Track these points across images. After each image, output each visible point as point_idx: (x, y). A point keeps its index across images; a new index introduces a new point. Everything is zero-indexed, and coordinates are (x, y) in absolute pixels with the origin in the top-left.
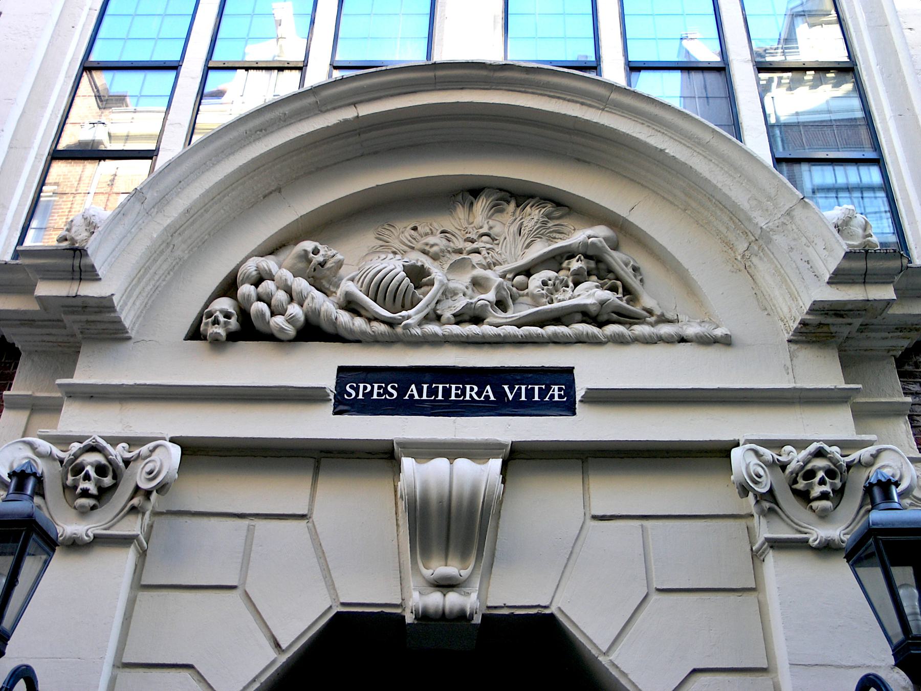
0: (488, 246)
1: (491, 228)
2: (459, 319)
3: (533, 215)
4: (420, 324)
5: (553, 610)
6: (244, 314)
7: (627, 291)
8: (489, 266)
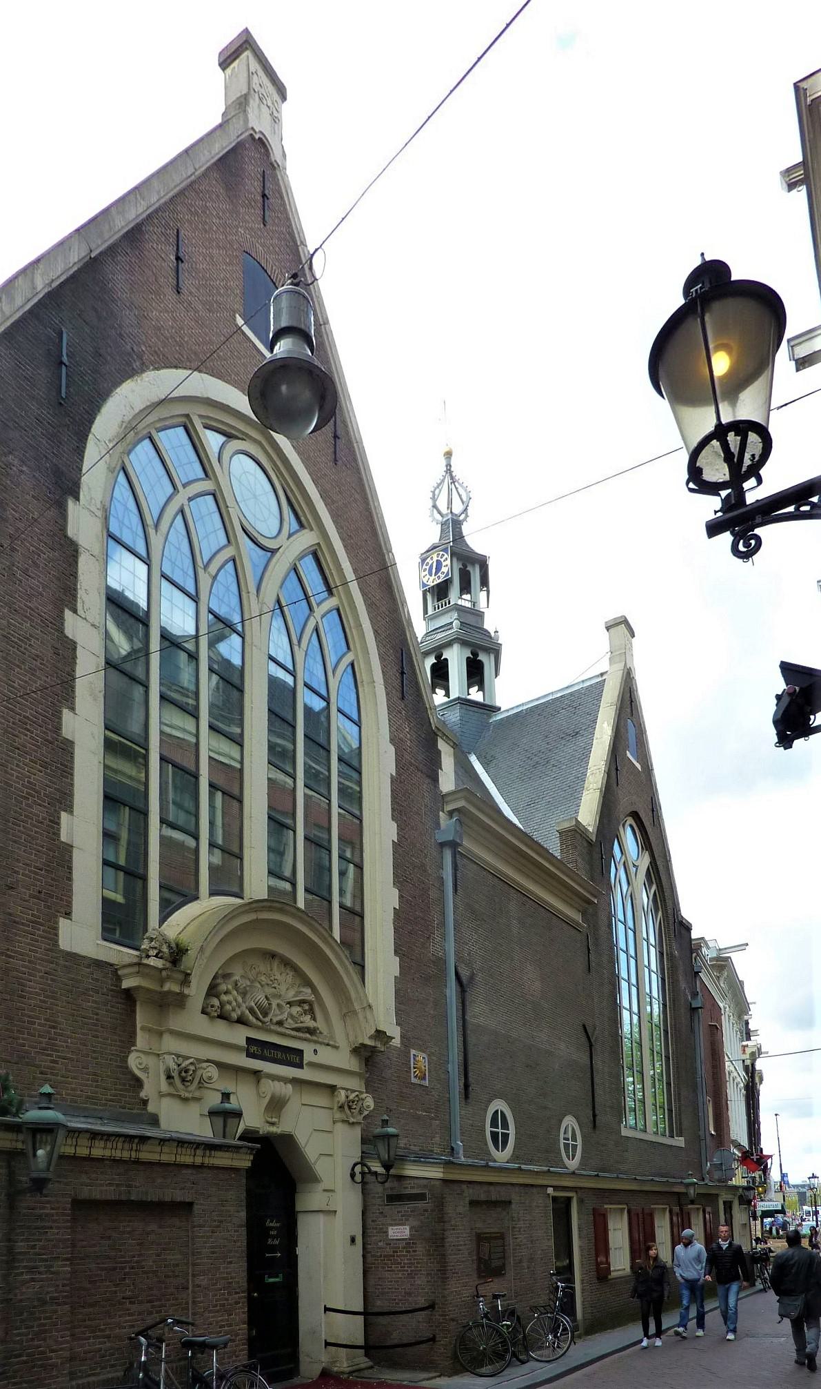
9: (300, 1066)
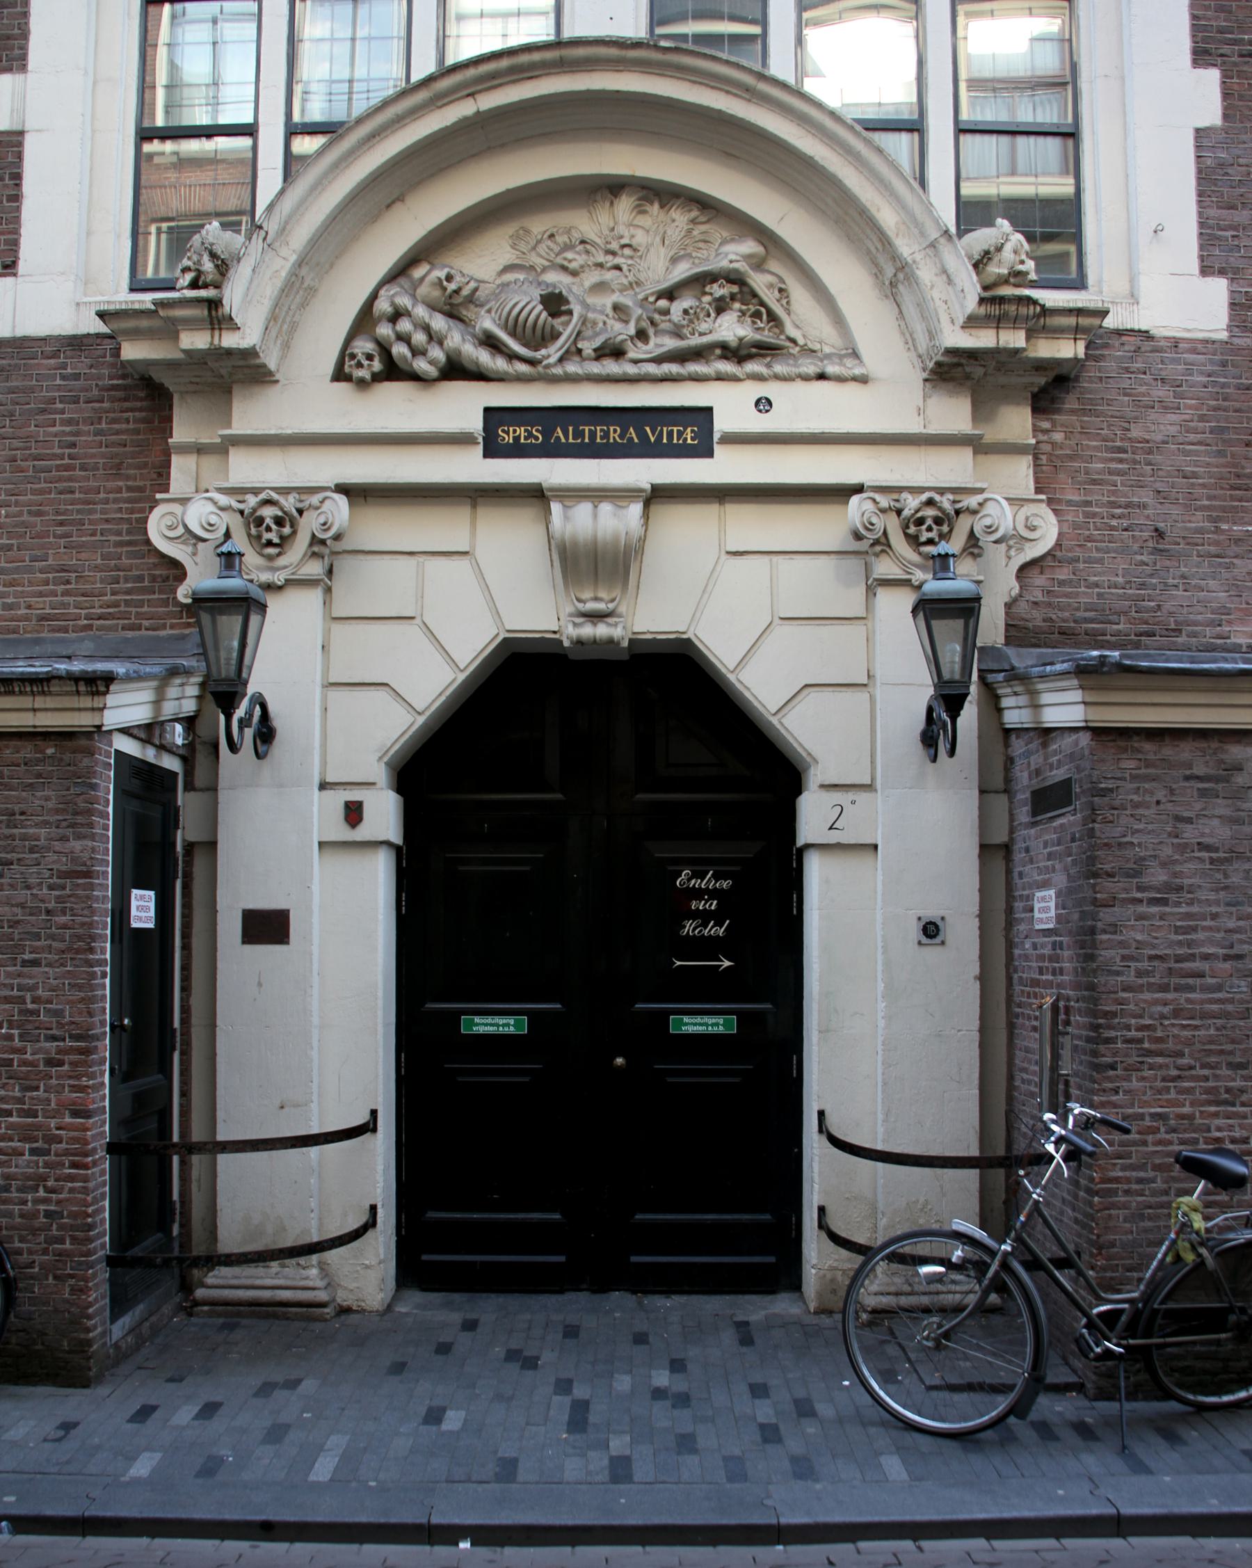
0: (630, 262)
2: (603, 353)
3: (679, 218)
4: (561, 360)
5: (690, 635)
6: (384, 350)
7: (773, 317)
9: (704, 450)
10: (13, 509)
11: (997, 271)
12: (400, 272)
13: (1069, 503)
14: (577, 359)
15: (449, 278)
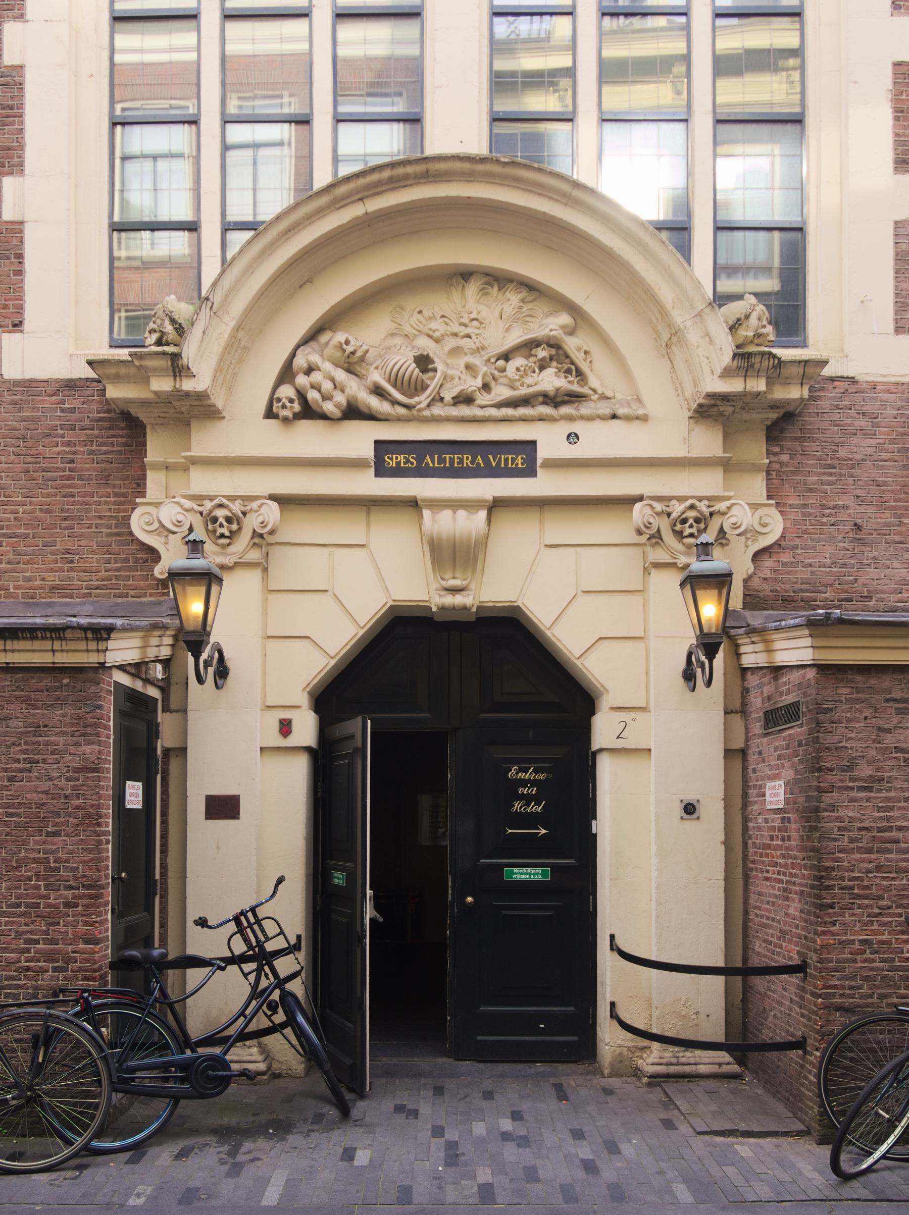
0: (477, 331)
1: (479, 313)
3: (513, 299)
4: (429, 406)
6: (302, 396)
7: (579, 373)
8: (477, 351)
10: (28, 508)
11: (745, 333)
12: (311, 337)
13: (792, 506)
14: (439, 404)
15: (347, 342)
